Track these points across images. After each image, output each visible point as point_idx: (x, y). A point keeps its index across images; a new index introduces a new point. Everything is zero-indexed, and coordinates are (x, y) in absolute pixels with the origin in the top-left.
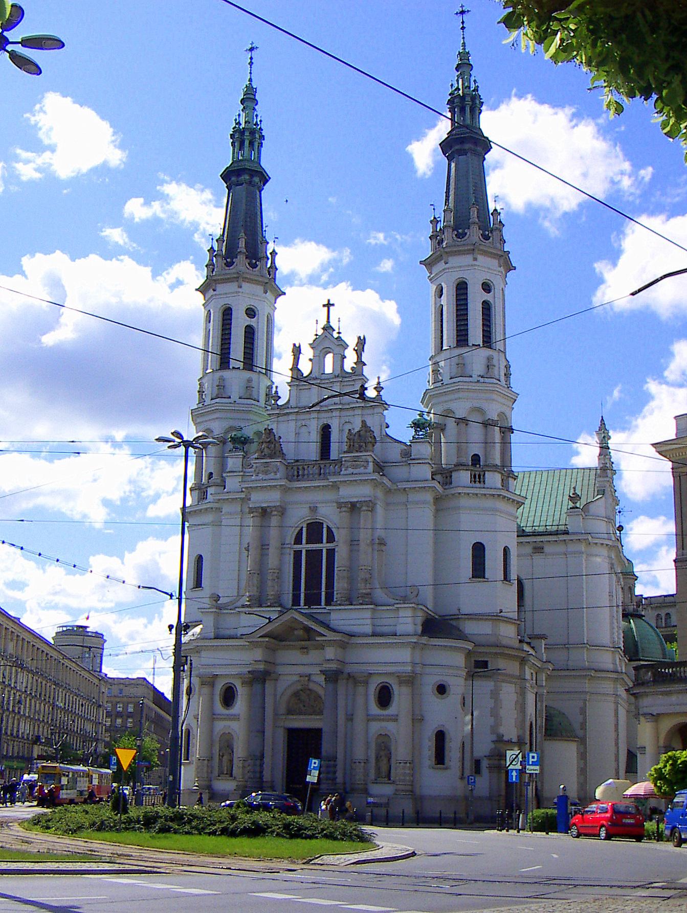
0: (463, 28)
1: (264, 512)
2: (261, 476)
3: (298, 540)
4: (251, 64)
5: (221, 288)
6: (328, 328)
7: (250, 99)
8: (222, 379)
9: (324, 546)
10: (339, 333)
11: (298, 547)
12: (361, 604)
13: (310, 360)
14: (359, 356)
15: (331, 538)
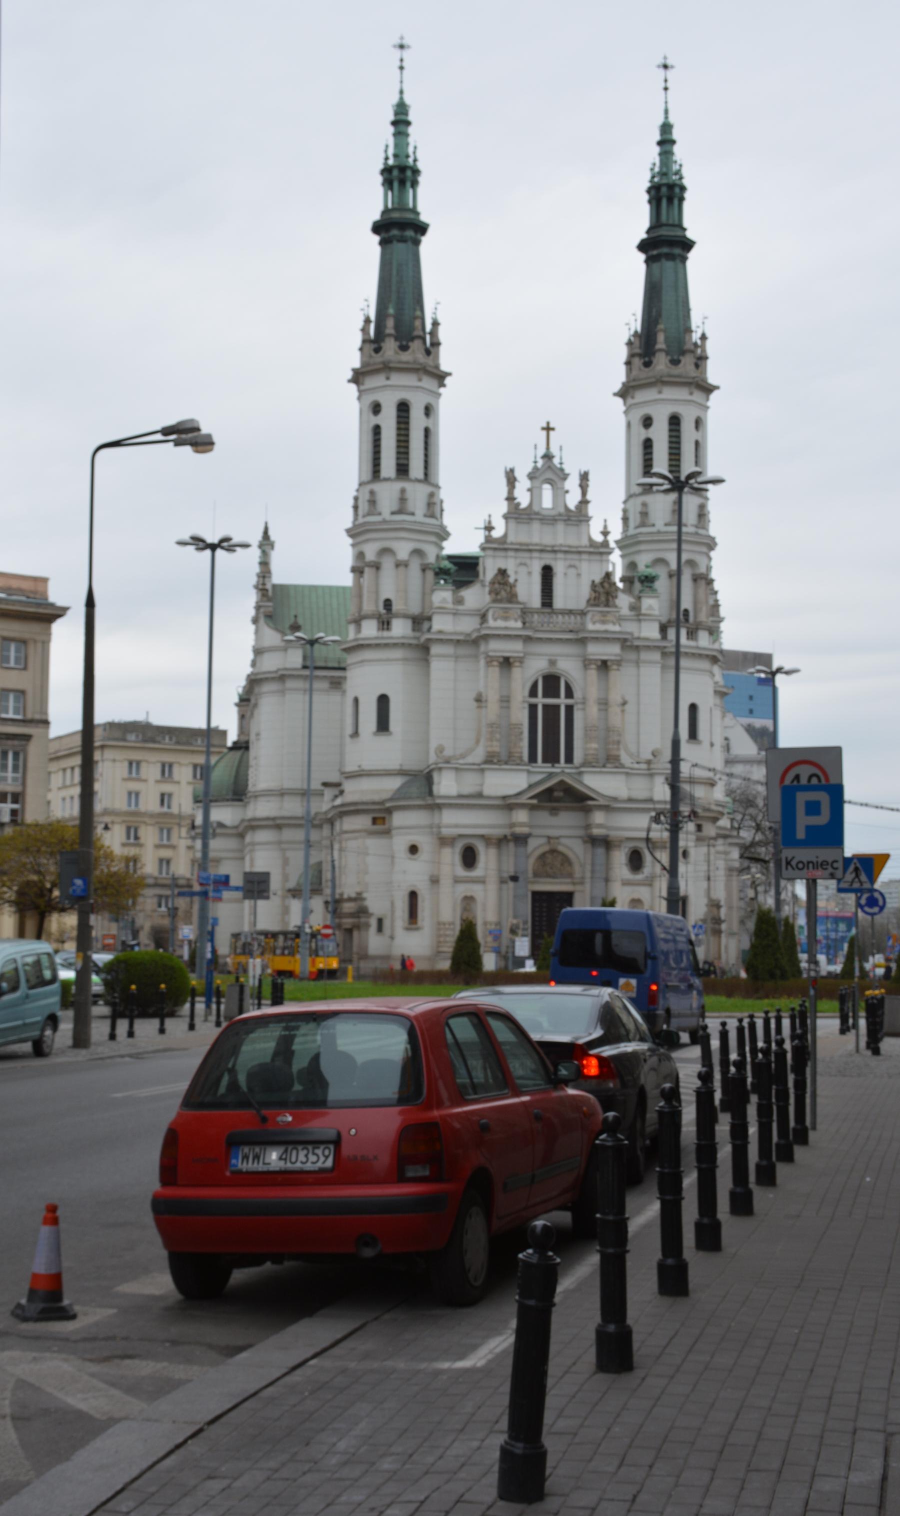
0: (666, 89)
1: (507, 663)
2: (500, 623)
3: (533, 692)
4: (401, 68)
5: (397, 379)
6: (548, 457)
7: (401, 122)
8: (403, 491)
9: (562, 701)
10: (561, 463)
11: (533, 700)
12: (616, 767)
13: (529, 490)
14: (584, 493)
15: (569, 694)
